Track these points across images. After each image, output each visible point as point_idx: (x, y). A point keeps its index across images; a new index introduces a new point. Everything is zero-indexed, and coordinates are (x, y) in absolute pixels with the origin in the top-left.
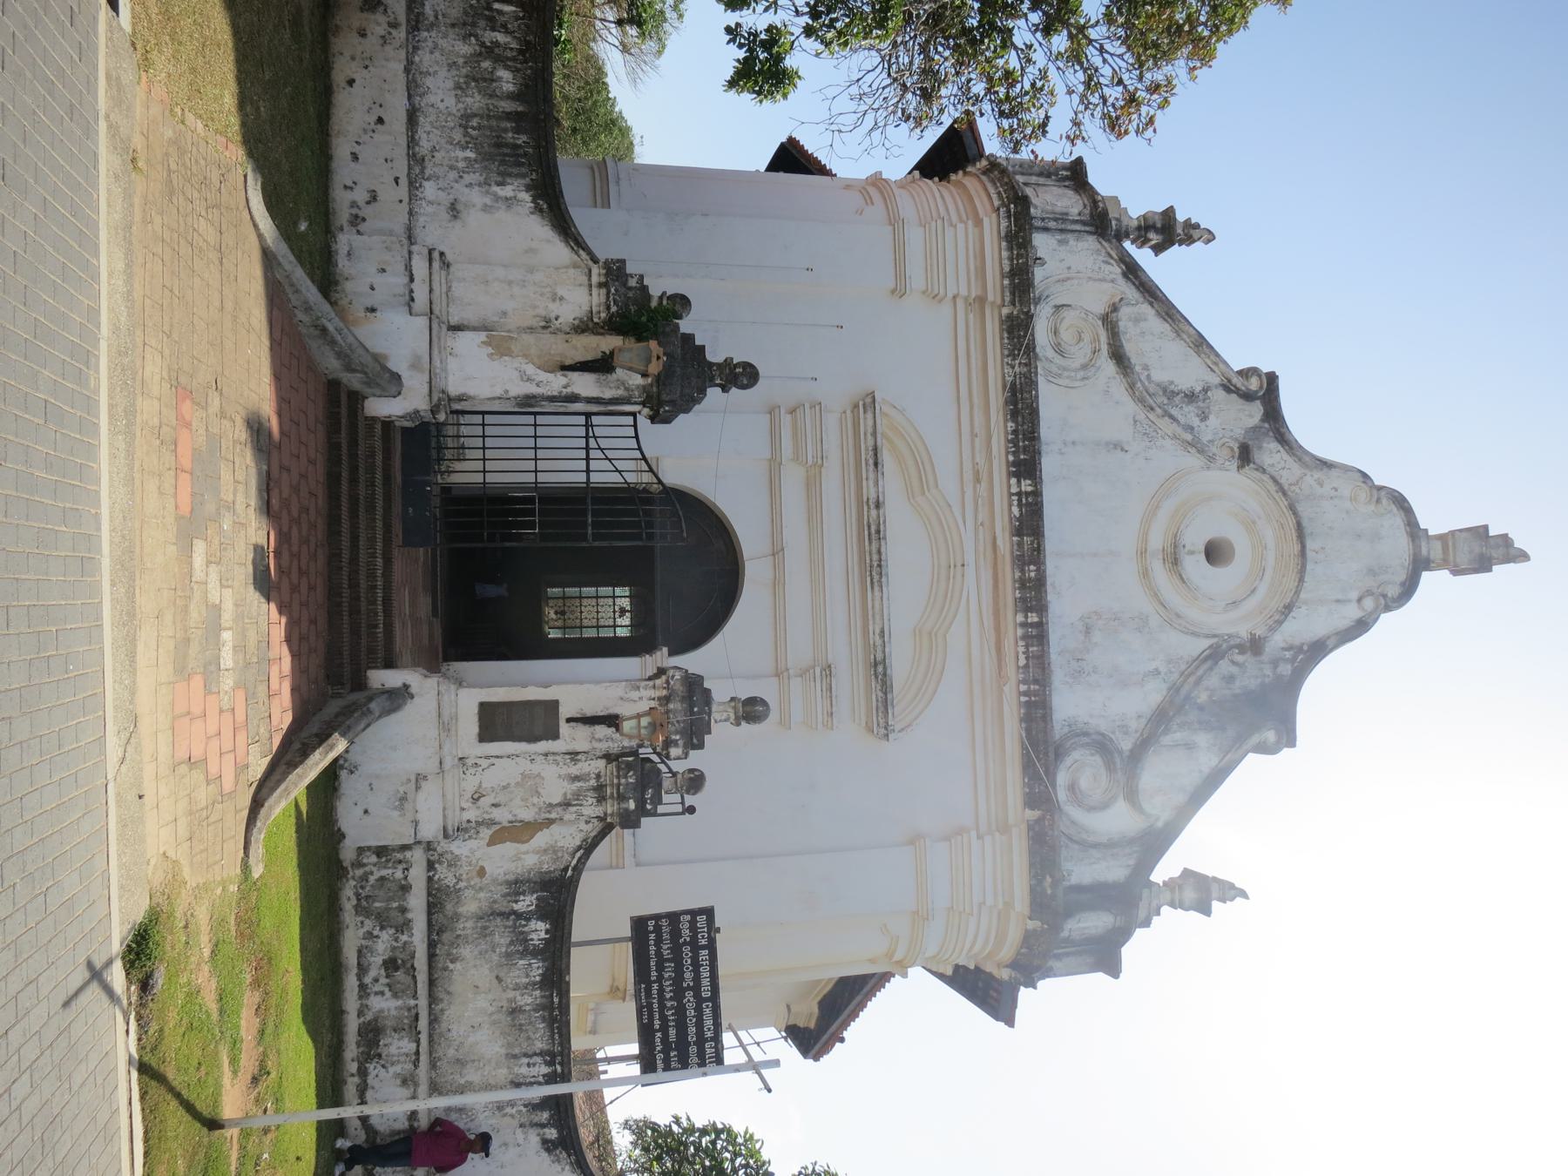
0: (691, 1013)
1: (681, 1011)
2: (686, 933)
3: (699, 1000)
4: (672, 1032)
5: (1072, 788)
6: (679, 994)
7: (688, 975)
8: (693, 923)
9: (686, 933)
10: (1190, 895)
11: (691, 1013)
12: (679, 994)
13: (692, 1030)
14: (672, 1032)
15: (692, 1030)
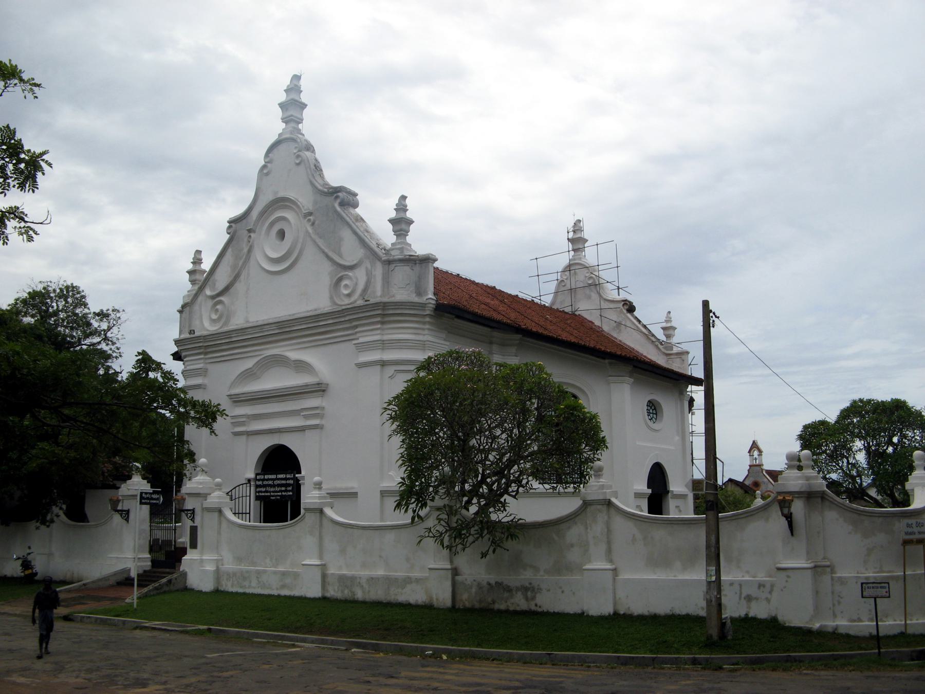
0: (279, 482)
1: (279, 485)
2: (260, 483)
3: (277, 479)
4: (283, 489)
5: (349, 295)
6: (274, 486)
7: (271, 482)
8: (259, 480)
9: (260, 483)
10: (404, 226)
11: (279, 482)
12: (274, 486)
13: (284, 482)
14: (283, 489)
15: (284, 482)
